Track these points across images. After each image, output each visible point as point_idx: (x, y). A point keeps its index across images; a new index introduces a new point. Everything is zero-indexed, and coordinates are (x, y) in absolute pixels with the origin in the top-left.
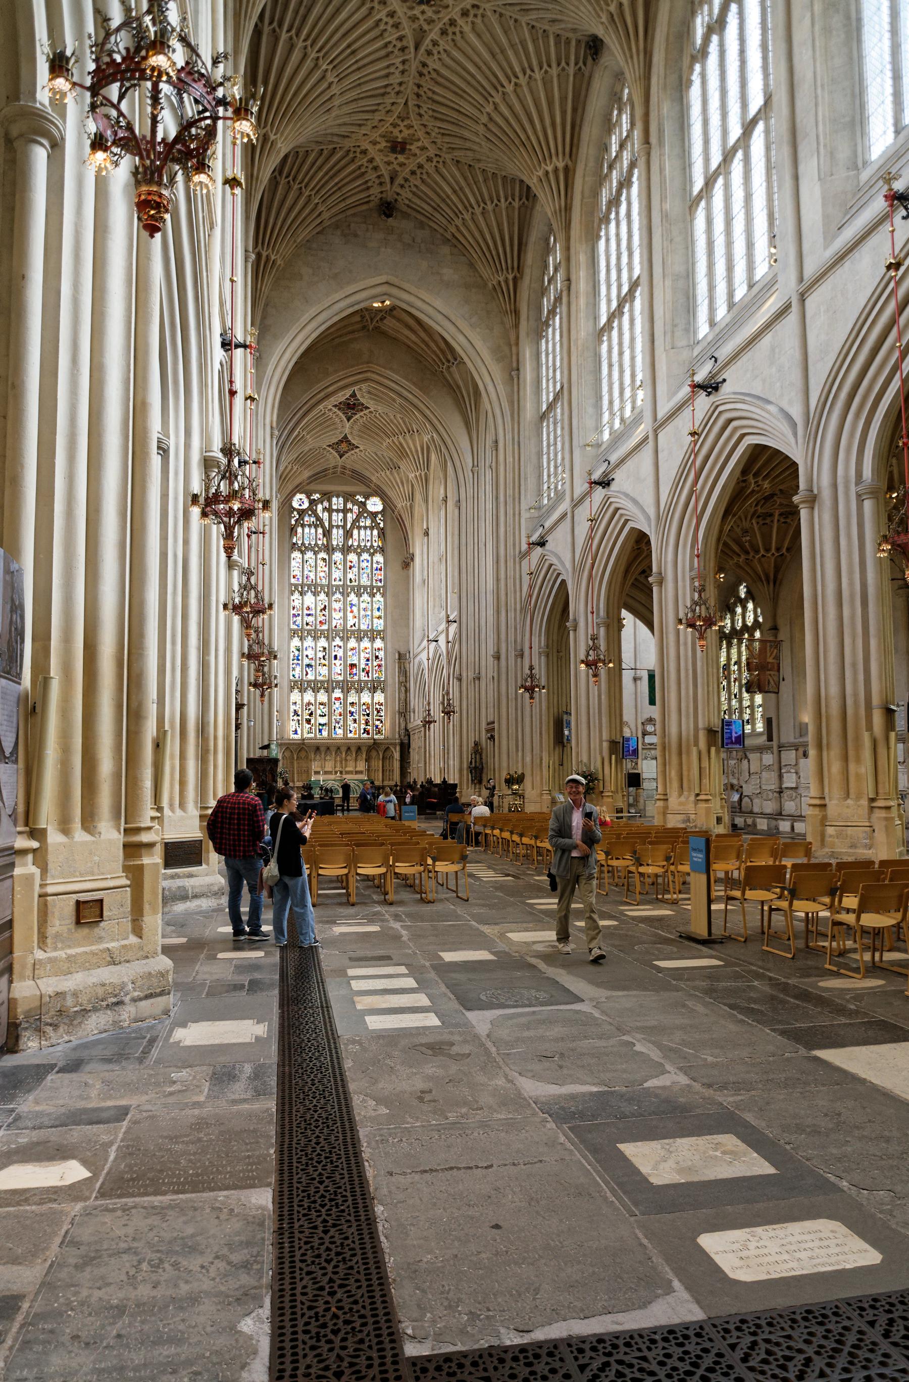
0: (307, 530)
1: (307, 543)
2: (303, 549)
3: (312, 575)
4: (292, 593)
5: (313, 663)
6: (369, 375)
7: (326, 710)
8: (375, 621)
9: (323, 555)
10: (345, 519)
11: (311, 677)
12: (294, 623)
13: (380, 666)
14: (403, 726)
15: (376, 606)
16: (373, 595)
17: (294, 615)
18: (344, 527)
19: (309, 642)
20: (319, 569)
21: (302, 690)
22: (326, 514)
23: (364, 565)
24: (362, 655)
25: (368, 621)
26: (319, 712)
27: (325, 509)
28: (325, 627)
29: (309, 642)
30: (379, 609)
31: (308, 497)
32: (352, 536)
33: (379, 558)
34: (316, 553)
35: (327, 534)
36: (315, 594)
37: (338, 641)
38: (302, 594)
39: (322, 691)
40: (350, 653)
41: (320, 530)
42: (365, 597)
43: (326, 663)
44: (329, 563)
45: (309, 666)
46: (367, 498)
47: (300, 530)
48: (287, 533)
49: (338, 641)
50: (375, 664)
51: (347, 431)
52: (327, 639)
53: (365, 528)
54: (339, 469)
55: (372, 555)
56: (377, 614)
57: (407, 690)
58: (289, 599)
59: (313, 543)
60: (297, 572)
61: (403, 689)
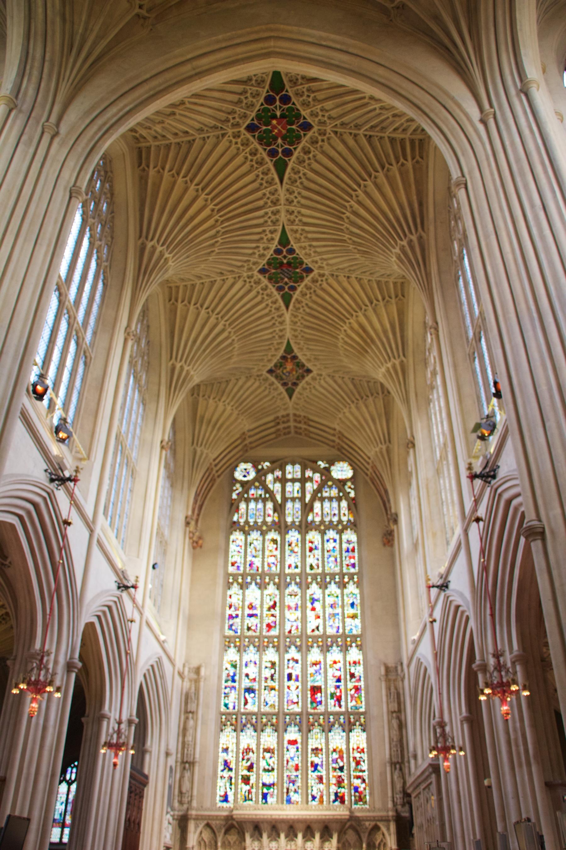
0: (252, 505)
1: (251, 521)
2: (246, 529)
3: (257, 562)
4: (229, 586)
5: (256, 686)
6: (272, 43)
7: (274, 762)
8: (348, 621)
9: (273, 535)
10: (303, 489)
11: (252, 707)
12: (231, 625)
13: (357, 689)
14: (399, 786)
15: (350, 601)
16: (342, 585)
17: (231, 617)
18: (302, 499)
19: (251, 655)
20: (267, 553)
21: (239, 728)
22: (278, 486)
23: (330, 545)
24: (330, 672)
25: (338, 623)
26: (263, 764)
27: (276, 480)
28: (274, 632)
29: (251, 655)
30: (352, 605)
31: (255, 466)
32: (311, 509)
33: (350, 536)
34: (263, 534)
35: (279, 509)
36: (262, 586)
37: (293, 653)
38: (243, 586)
39: (269, 730)
40: (311, 670)
41: (270, 505)
42: (333, 588)
43: (276, 685)
44: (282, 545)
45: (249, 690)
46: (332, 463)
47: (243, 506)
48: (226, 508)
49: (293, 653)
50: (350, 685)
51: (288, 334)
52: (277, 648)
53: (330, 499)
54: (292, 424)
55: (340, 532)
56: (351, 611)
57: (402, 726)
58: (224, 594)
59: (260, 520)
60: (239, 559)
61: (395, 723)
